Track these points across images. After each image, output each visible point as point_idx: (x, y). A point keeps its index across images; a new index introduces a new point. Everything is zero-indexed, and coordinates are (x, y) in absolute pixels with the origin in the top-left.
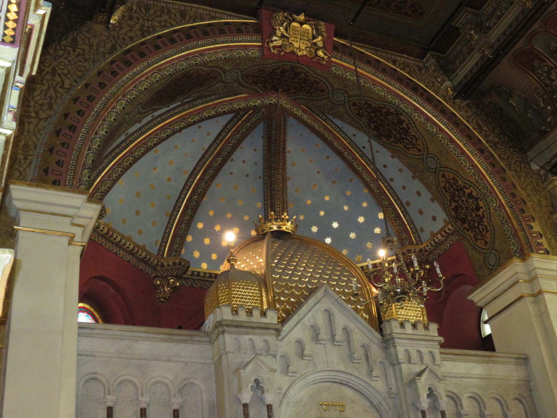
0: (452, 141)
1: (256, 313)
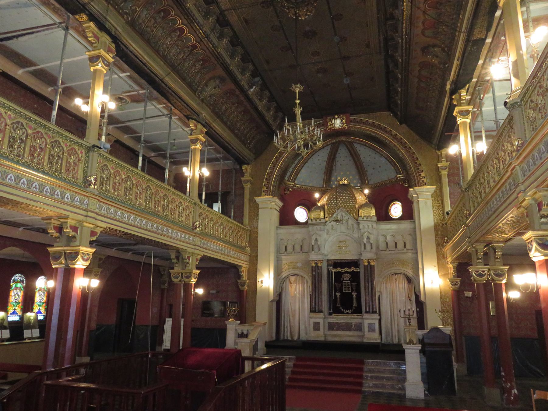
0: (395, 145)
1: (318, 220)
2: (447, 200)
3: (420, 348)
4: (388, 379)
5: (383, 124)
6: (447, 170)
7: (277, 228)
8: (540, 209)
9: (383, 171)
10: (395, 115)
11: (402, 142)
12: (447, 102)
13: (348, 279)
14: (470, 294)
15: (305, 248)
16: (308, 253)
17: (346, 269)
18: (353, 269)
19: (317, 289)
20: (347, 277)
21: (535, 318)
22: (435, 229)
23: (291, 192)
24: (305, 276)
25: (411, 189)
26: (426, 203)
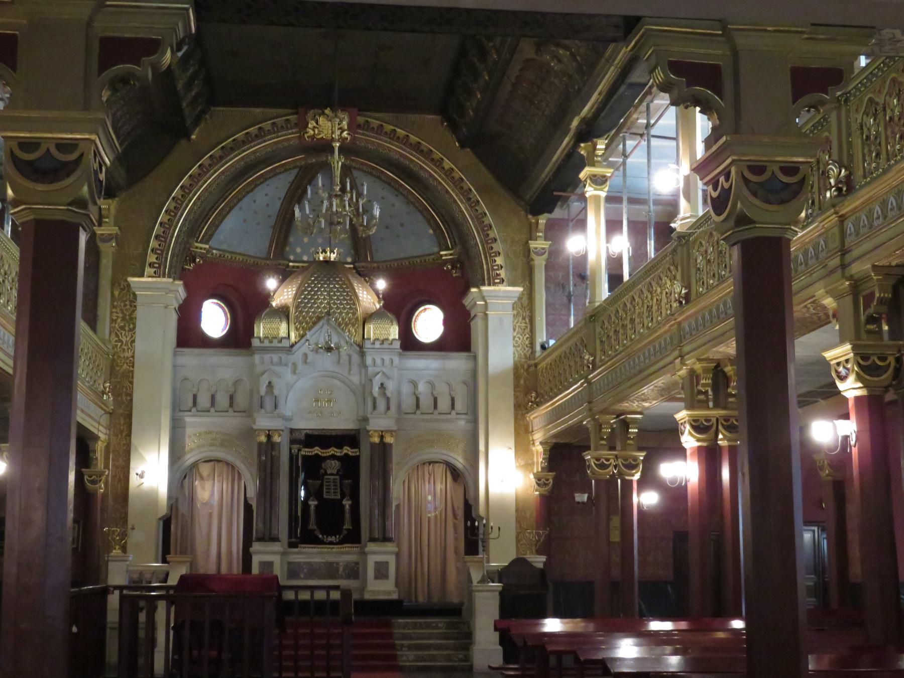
0: (447, 192)
2: (542, 319)
3: (500, 589)
4: (439, 647)
5: (450, 168)
6: (546, 256)
7: (175, 354)
8: (698, 384)
9: (419, 243)
10: (454, 127)
11: (462, 188)
12: (568, 144)
13: (335, 472)
14: (585, 497)
15: (242, 400)
16: (248, 413)
17: (332, 451)
18: (347, 450)
19: (268, 492)
20: (333, 467)
21: (671, 546)
22: (514, 374)
23: (198, 266)
24: (239, 464)
25: (474, 290)
26: (501, 320)
